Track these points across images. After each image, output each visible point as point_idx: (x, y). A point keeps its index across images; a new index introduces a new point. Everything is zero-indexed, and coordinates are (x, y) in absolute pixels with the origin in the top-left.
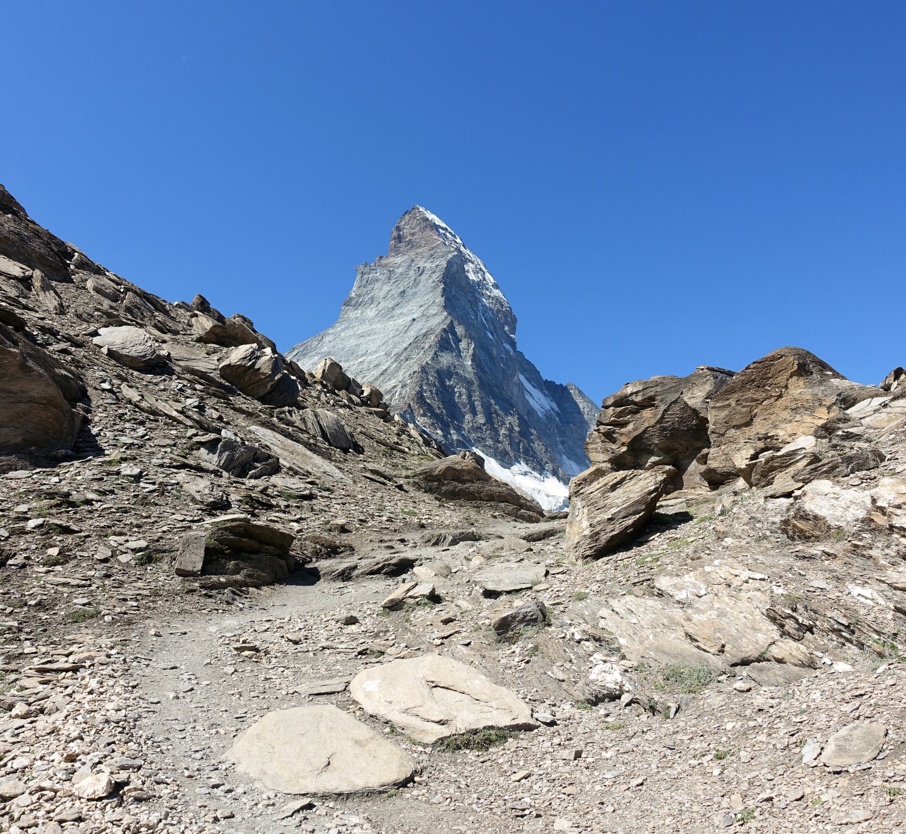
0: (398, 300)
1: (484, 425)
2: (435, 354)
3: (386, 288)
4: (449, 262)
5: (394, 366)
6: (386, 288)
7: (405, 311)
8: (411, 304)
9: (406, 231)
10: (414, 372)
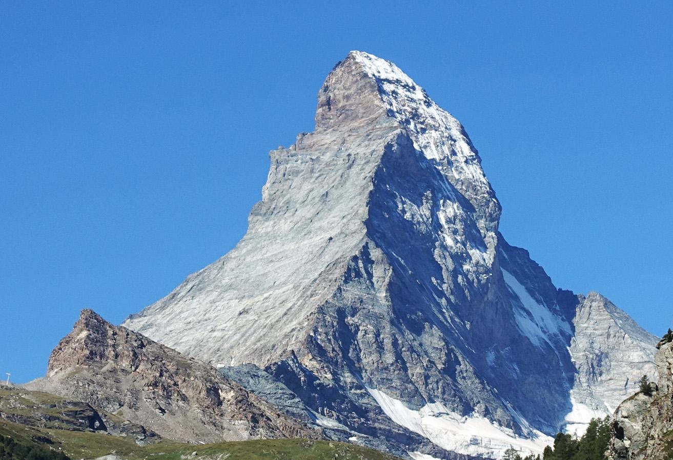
0: (319, 206)
1: (392, 365)
2: (339, 289)
3: (307, 186)
4: (388, 147)
6: (307, 186)
7: (324, 223)
8: (333, 213)
9: (337, 93)
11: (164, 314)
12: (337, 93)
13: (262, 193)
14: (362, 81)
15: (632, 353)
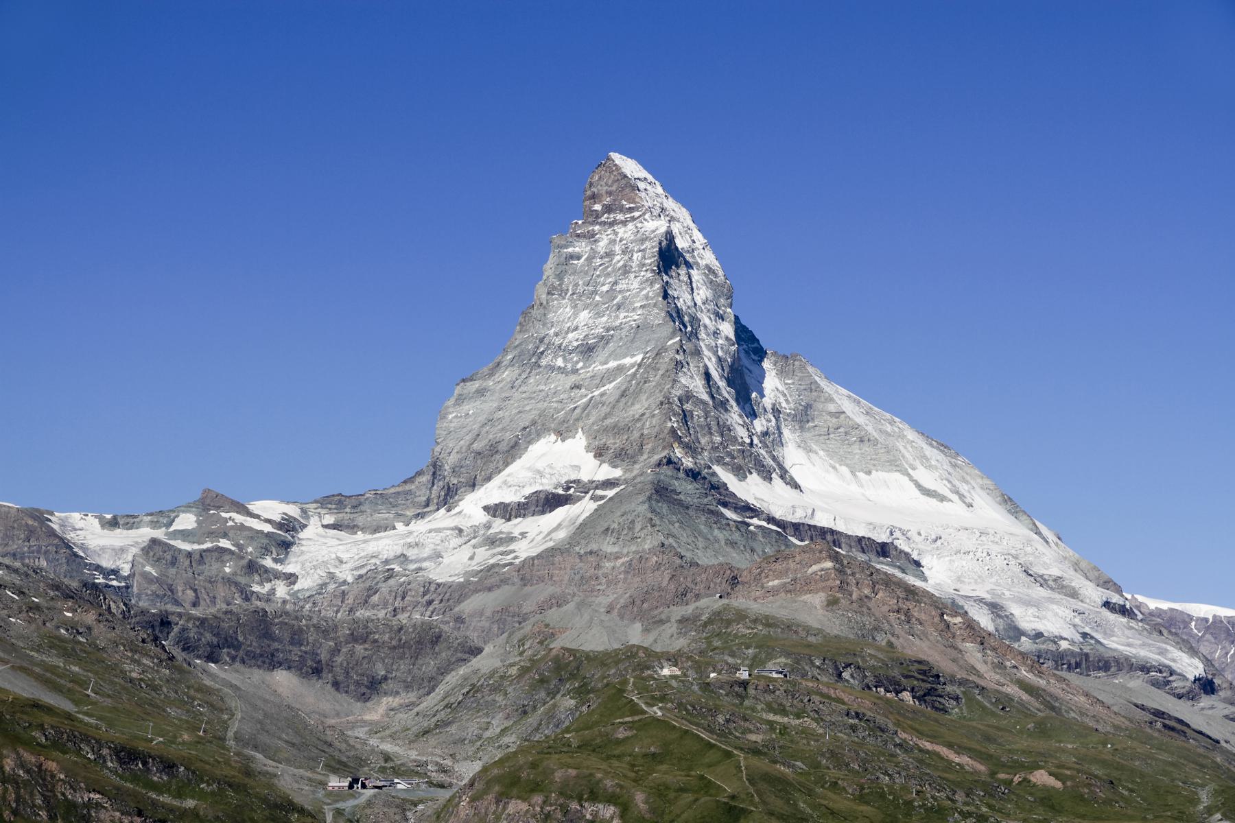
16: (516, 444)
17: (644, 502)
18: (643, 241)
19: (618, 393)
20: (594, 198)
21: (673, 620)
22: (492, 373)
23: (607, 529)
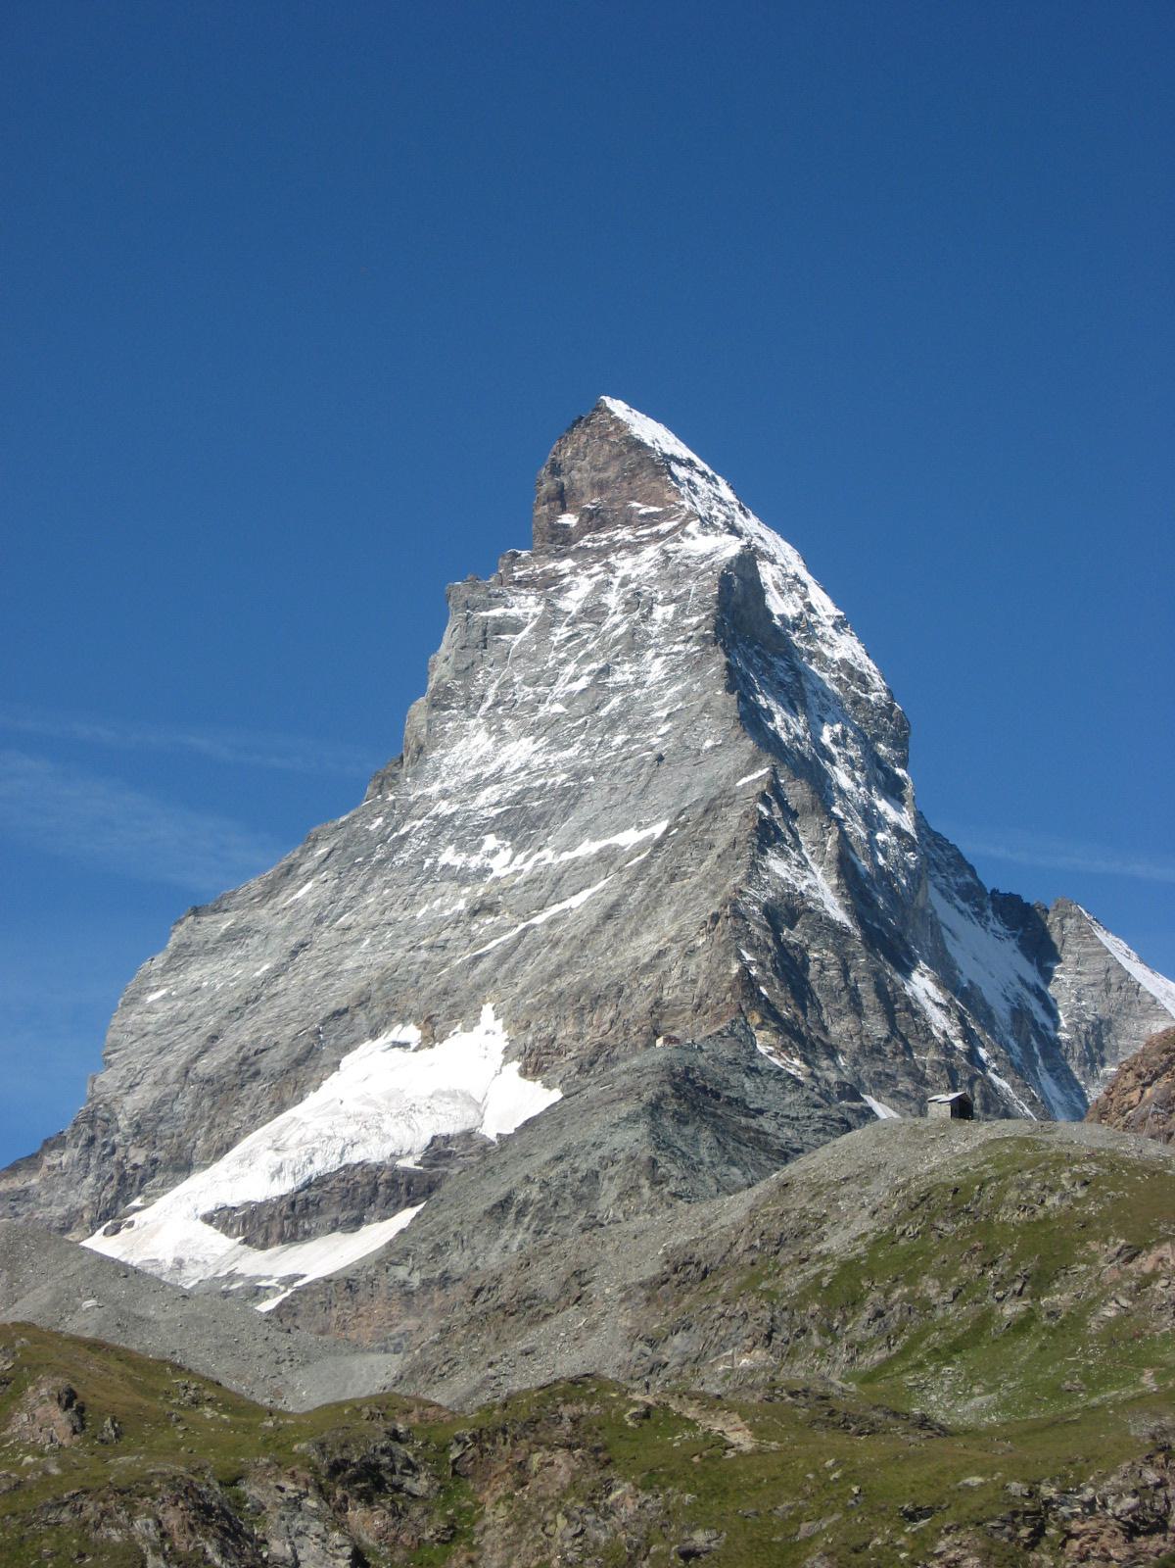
1: (888, 1041)
2: (753, 864)
5: (639, 892)
10: (715, 918)
11: (273, 908)
12: (577, 477)
13: (430, 670)
14: (633, 454)
15: (1155, 1023)
16: (310, 1053)
17: (632, 1119)
18: (676, 578)
19: (597, 911)
20: (562, 498)
21: (605, 1288)
22: (270, 892)
23: (504, 1204)
